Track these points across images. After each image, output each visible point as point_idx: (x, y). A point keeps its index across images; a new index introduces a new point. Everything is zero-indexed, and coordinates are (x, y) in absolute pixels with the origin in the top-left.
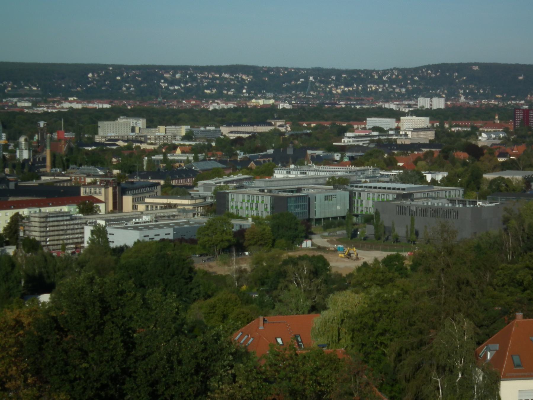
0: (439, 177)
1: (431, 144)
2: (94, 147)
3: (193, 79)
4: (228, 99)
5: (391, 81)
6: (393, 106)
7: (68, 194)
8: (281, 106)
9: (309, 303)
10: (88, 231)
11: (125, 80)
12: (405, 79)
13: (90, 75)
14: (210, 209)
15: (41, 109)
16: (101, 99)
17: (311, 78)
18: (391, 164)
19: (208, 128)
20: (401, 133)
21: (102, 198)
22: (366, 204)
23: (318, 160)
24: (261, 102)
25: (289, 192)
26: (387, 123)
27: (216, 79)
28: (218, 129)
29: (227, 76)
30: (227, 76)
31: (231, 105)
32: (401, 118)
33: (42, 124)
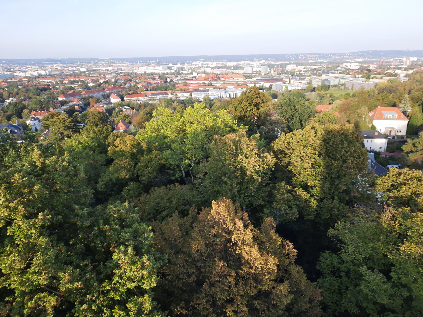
0: (360, 76)
1: (359, 69)
3: (306, 56)
4: (313, 60)
5: (350, 55)
6: (350, 61)
7: (280, 80)
8: (324, 61)
9: (329, 102)
10: (284, 87)
11: (292, 57)
14: (309, 83)
15: (275, 63)
16: (287, 61)
18: (348, 73)
22: (342, 82)
23: (332, 73)
24: (320, 61)
31: (314, 62)
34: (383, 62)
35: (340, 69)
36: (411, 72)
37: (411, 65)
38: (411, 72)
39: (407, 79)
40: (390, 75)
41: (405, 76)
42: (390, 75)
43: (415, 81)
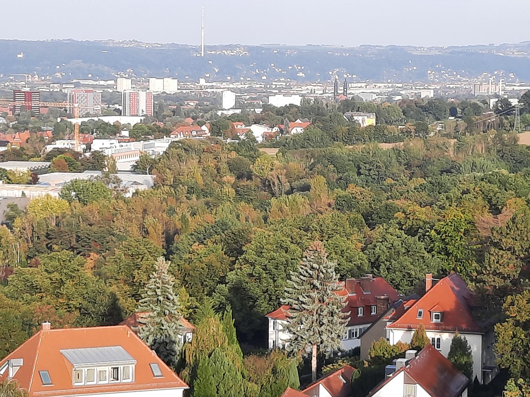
34: (28, 96)
36: (160, 146)
37: (158, 114)
38: (160, 146)
39: (145, 181)
40: (71, 162)
41: (137, 169)
42: (71, 162)
43: (183, 189)
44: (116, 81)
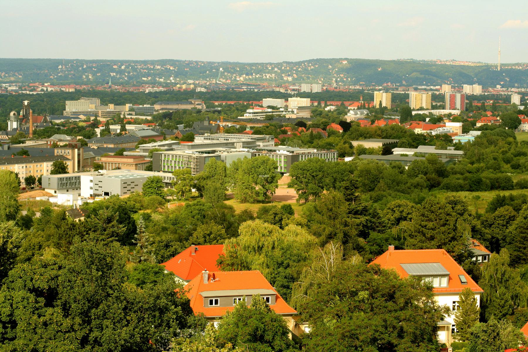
2: (62, 120)
12: (291, 70)
13: (60, 67)
17: (221, 69)
19: (145, 106)
20: (289, 110)
21: (70, 157)
25: (206, 153)
26: (278, 102)
27: (151, 69)
28: (152, 106)
29: (159, 67)
30: (159, 67)
32: (289, 99)
33: (26, 102)
35: (251, 116)
44: (441, 86)
